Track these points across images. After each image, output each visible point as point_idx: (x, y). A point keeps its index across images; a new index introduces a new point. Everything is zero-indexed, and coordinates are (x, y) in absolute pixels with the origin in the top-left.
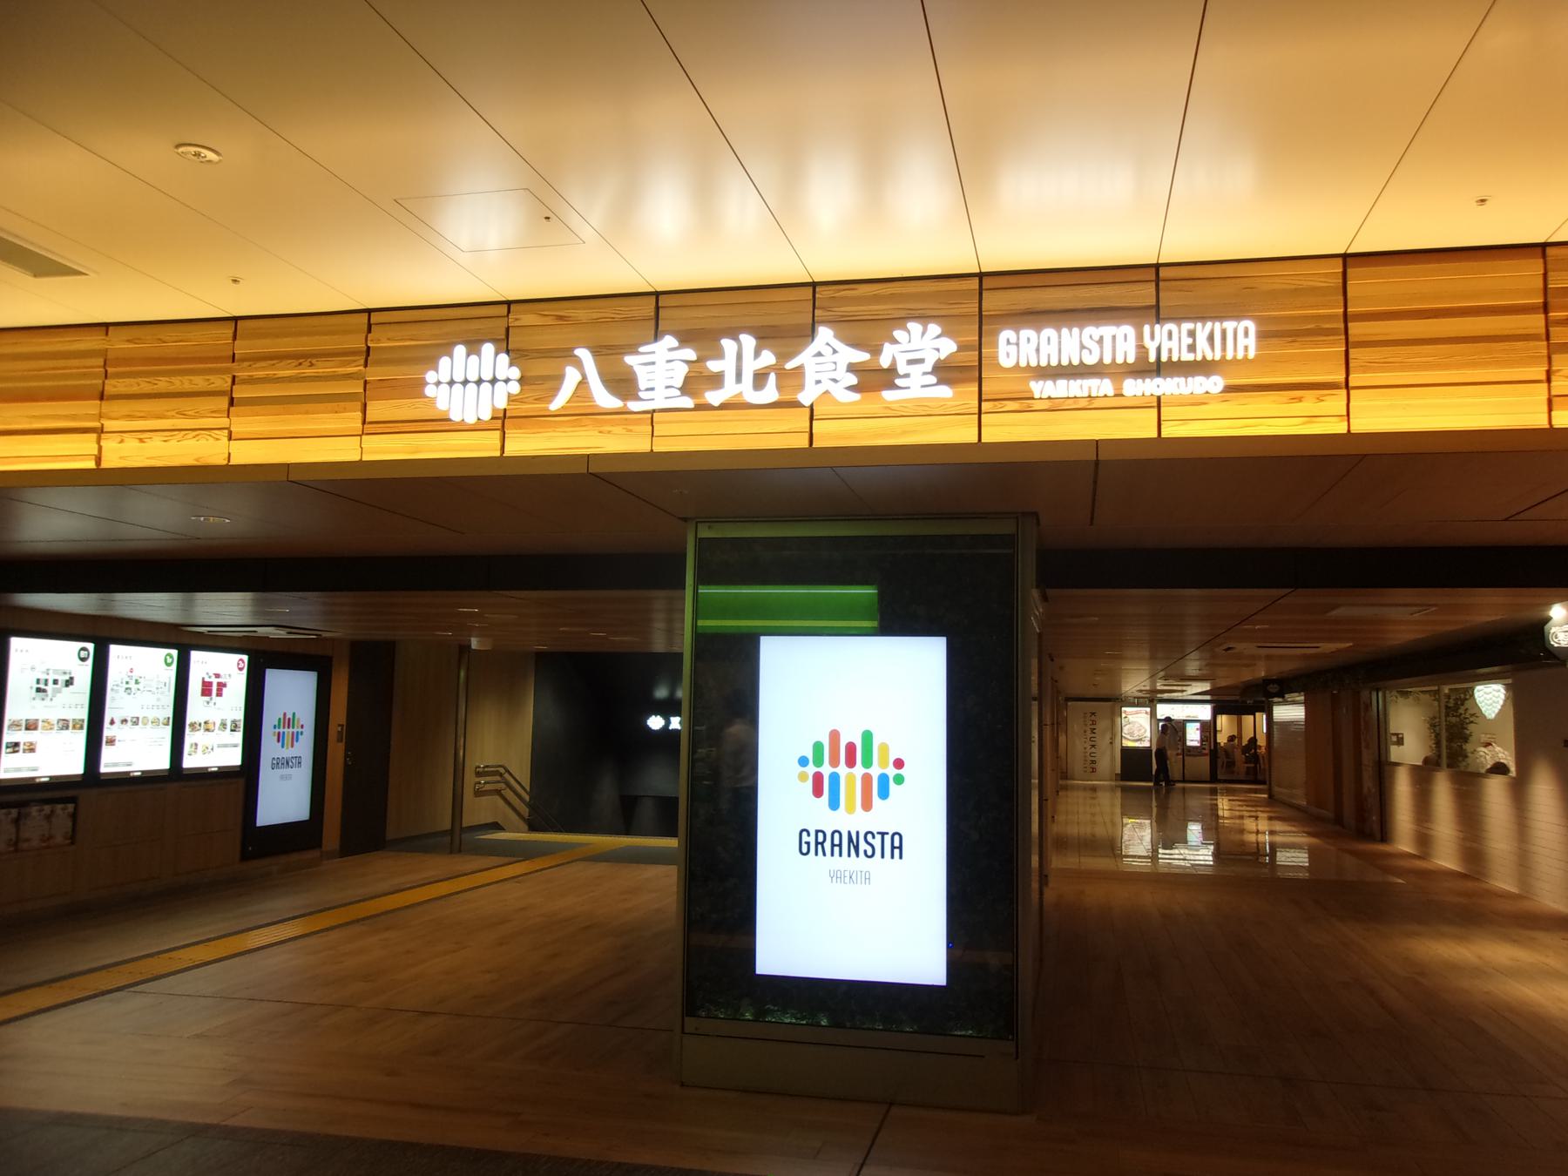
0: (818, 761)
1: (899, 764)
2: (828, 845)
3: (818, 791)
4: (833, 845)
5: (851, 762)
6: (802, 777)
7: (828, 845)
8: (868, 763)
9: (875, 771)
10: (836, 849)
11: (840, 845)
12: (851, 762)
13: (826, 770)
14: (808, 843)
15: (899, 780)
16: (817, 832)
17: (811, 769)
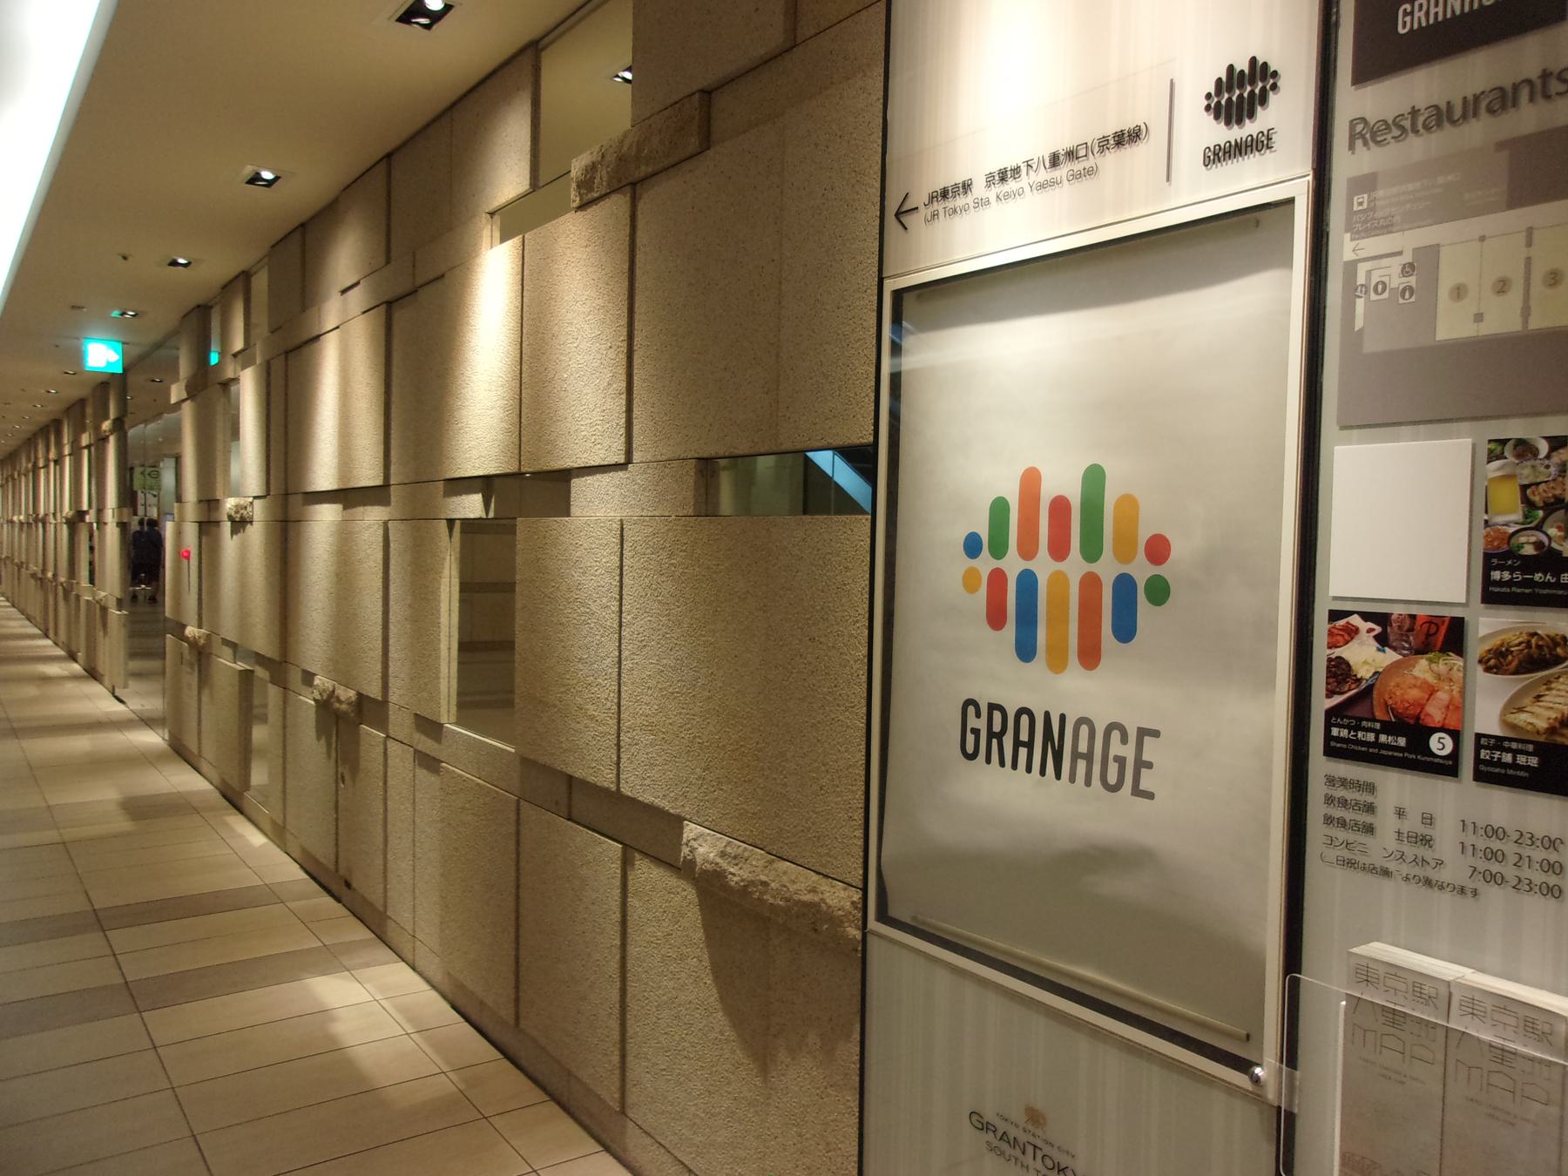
0: (999, 550)
1: (1158, 550)
2: (1008, 741)
3: (996, 618)
4: (1017, 743)
5: (1059, 550)
6: (970, 581)
7: (1008, 741)
8: (1092, 551)
9: (1107, 569)
10: (1023, 752)
11: (1030, 745)
12: (1059, 550)
13: (1013, 565)
14: (976, 732)
15: (1159, 592)
16: (992, 707)
17: (985, 564)
